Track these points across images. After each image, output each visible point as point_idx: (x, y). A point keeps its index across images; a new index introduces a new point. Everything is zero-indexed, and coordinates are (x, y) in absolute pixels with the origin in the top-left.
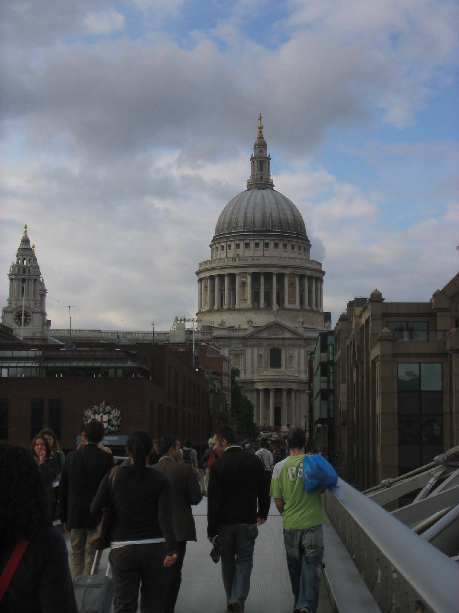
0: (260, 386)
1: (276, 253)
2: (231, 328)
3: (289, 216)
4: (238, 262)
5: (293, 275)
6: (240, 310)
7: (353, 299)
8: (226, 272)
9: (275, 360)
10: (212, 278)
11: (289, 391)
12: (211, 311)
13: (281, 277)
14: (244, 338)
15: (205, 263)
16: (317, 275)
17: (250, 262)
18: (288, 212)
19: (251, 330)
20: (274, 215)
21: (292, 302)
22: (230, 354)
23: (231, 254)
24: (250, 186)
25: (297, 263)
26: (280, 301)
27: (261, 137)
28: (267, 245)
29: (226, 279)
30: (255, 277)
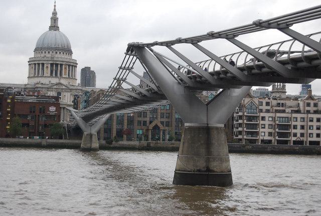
5: (66, 65)
6: (45, 77)
10: (35, 64)
12: (34, 77)
13: (61, 65)
14: (48, 88)
15: (32, 58)
17: (50, 59)
18: (64, 40)
21: (65, 74)
23: (42, 55)
25: (68, 60)
26: (61, 74)
27: (55, 10)
28: (56, 53)
29: (41, 65)
30: (52, 65)
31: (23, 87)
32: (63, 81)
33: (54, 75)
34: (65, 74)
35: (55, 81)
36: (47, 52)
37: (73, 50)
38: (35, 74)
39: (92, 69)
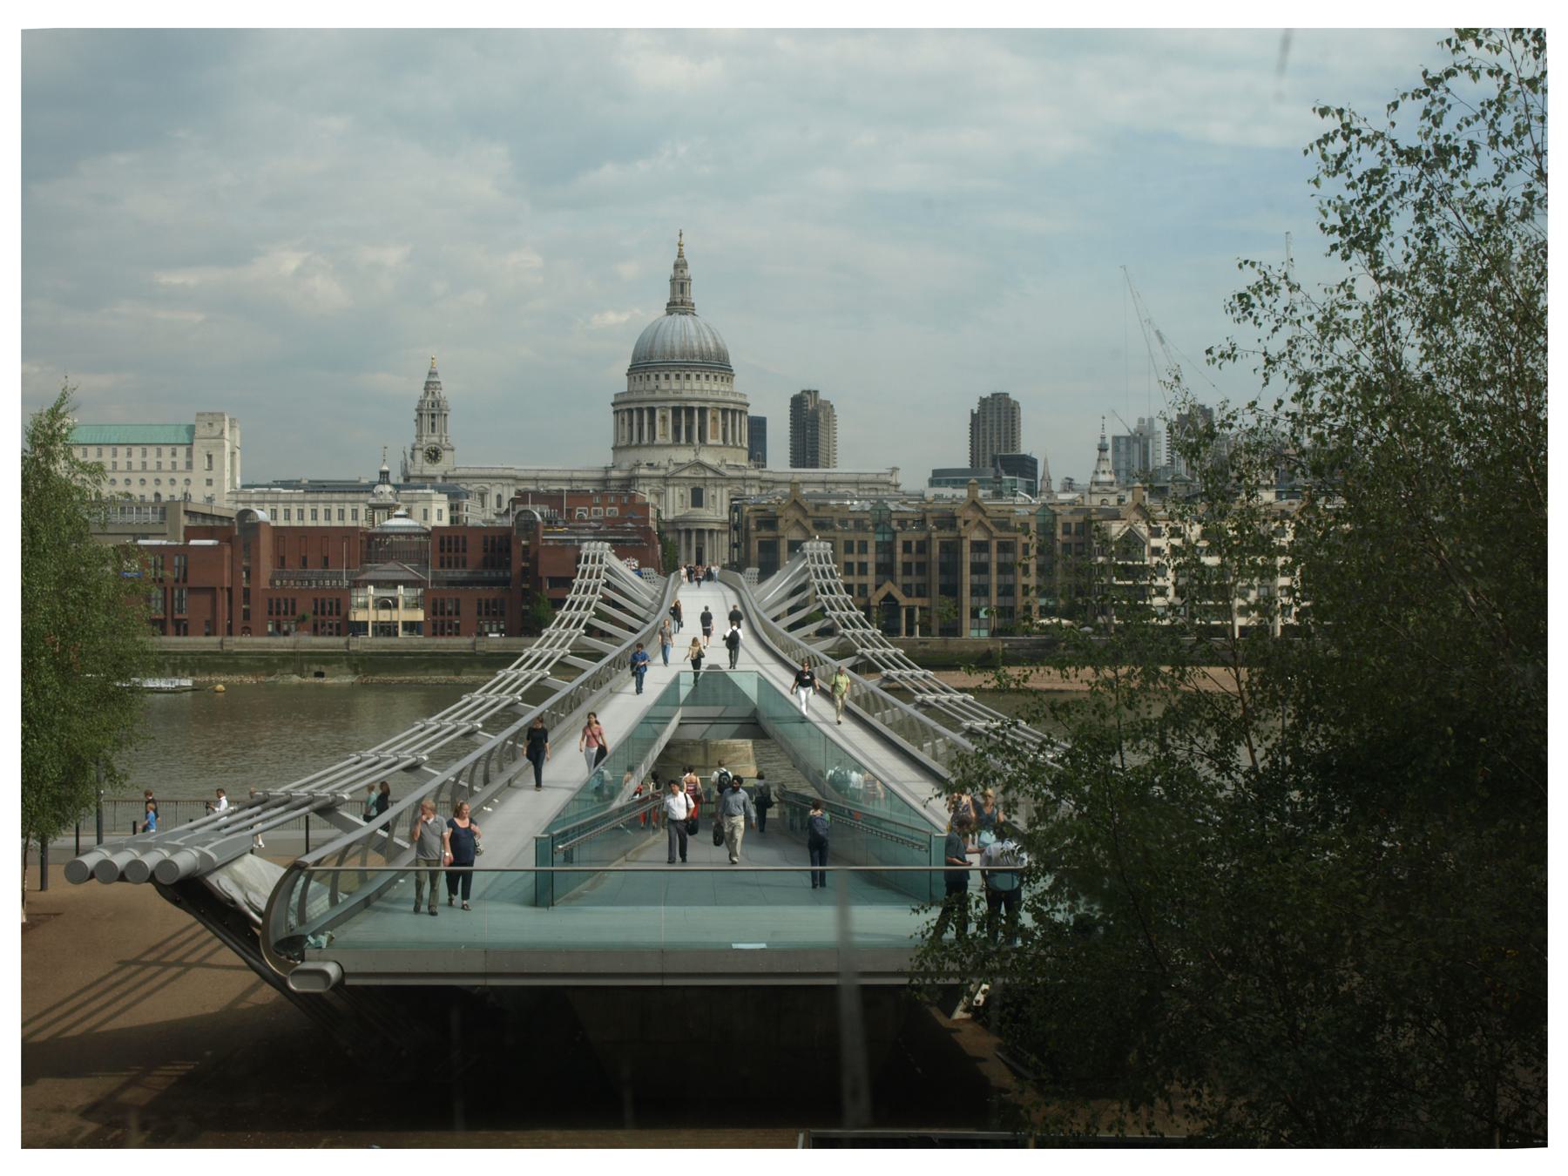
0: (682, 527)
1: (696, 386)
2: (650, 465)
3: (712, 345)
4: (658, 395)
6: (660, 446)
7: (798, 392)
8: (645, 405)
9: (697, 499)
10: (630, 411)
11: (711, 531)
12: (629, 447)
13: (702, 411)
14: (665, 478)
16: (739, 407)
17: (671, 395)
18: (710, 340)
19: (672, 469)
20: (696, 344)
22: (651, 493)
24: (670, 312)
25: (720, 397)
28: (688, 377)
30: (676, 411)
31: (600, 475)
32: (708, 458)
33: (683, 441)
34: (715, 437)
35: (684, 455)
36: (662, 377)
37: (733, 362)
38: (631, 439)
39: (822, 396)
